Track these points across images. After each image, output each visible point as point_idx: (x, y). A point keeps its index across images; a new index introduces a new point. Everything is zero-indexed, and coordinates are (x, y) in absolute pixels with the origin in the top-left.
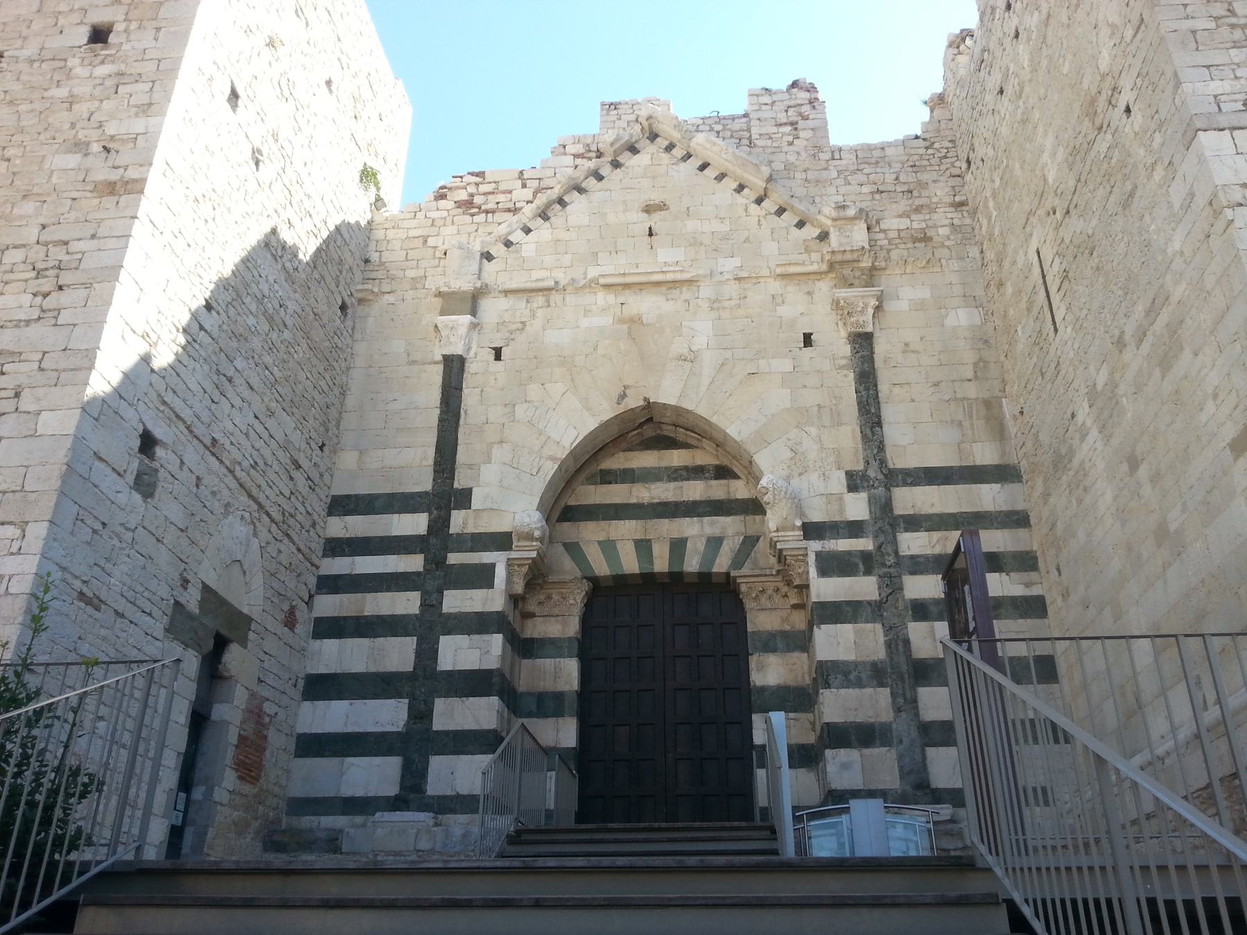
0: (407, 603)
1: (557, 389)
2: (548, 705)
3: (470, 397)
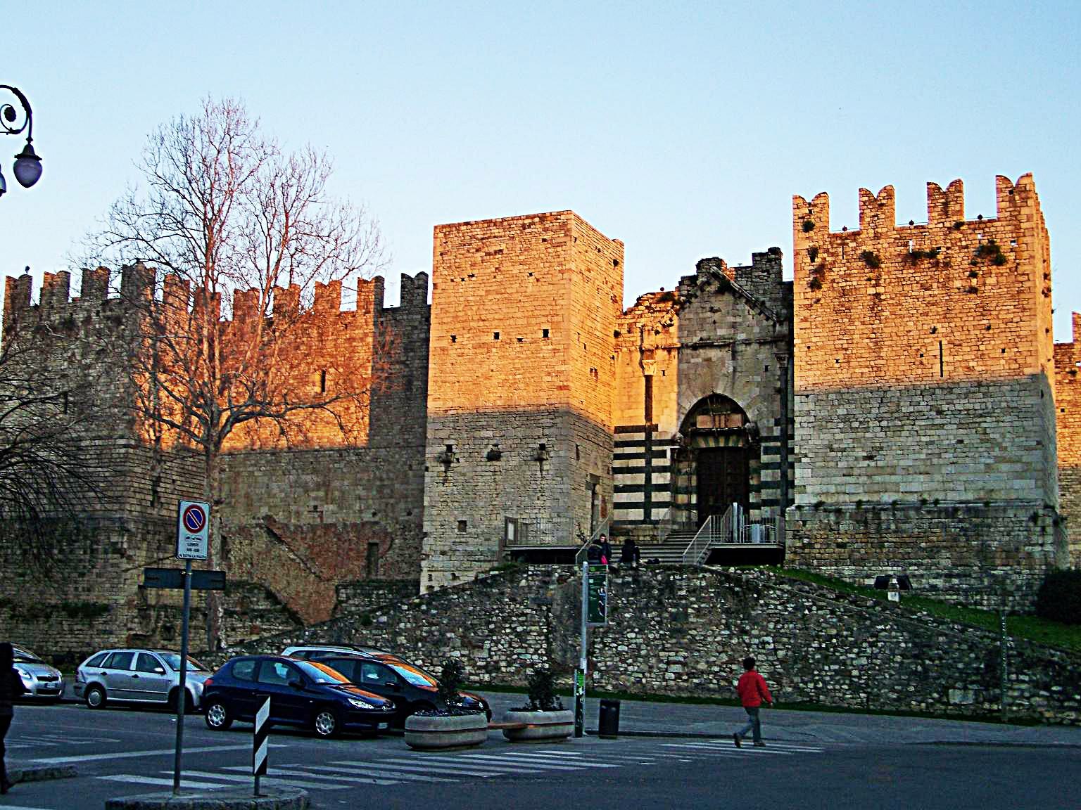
0: (641, 463)
3: (655, 390)
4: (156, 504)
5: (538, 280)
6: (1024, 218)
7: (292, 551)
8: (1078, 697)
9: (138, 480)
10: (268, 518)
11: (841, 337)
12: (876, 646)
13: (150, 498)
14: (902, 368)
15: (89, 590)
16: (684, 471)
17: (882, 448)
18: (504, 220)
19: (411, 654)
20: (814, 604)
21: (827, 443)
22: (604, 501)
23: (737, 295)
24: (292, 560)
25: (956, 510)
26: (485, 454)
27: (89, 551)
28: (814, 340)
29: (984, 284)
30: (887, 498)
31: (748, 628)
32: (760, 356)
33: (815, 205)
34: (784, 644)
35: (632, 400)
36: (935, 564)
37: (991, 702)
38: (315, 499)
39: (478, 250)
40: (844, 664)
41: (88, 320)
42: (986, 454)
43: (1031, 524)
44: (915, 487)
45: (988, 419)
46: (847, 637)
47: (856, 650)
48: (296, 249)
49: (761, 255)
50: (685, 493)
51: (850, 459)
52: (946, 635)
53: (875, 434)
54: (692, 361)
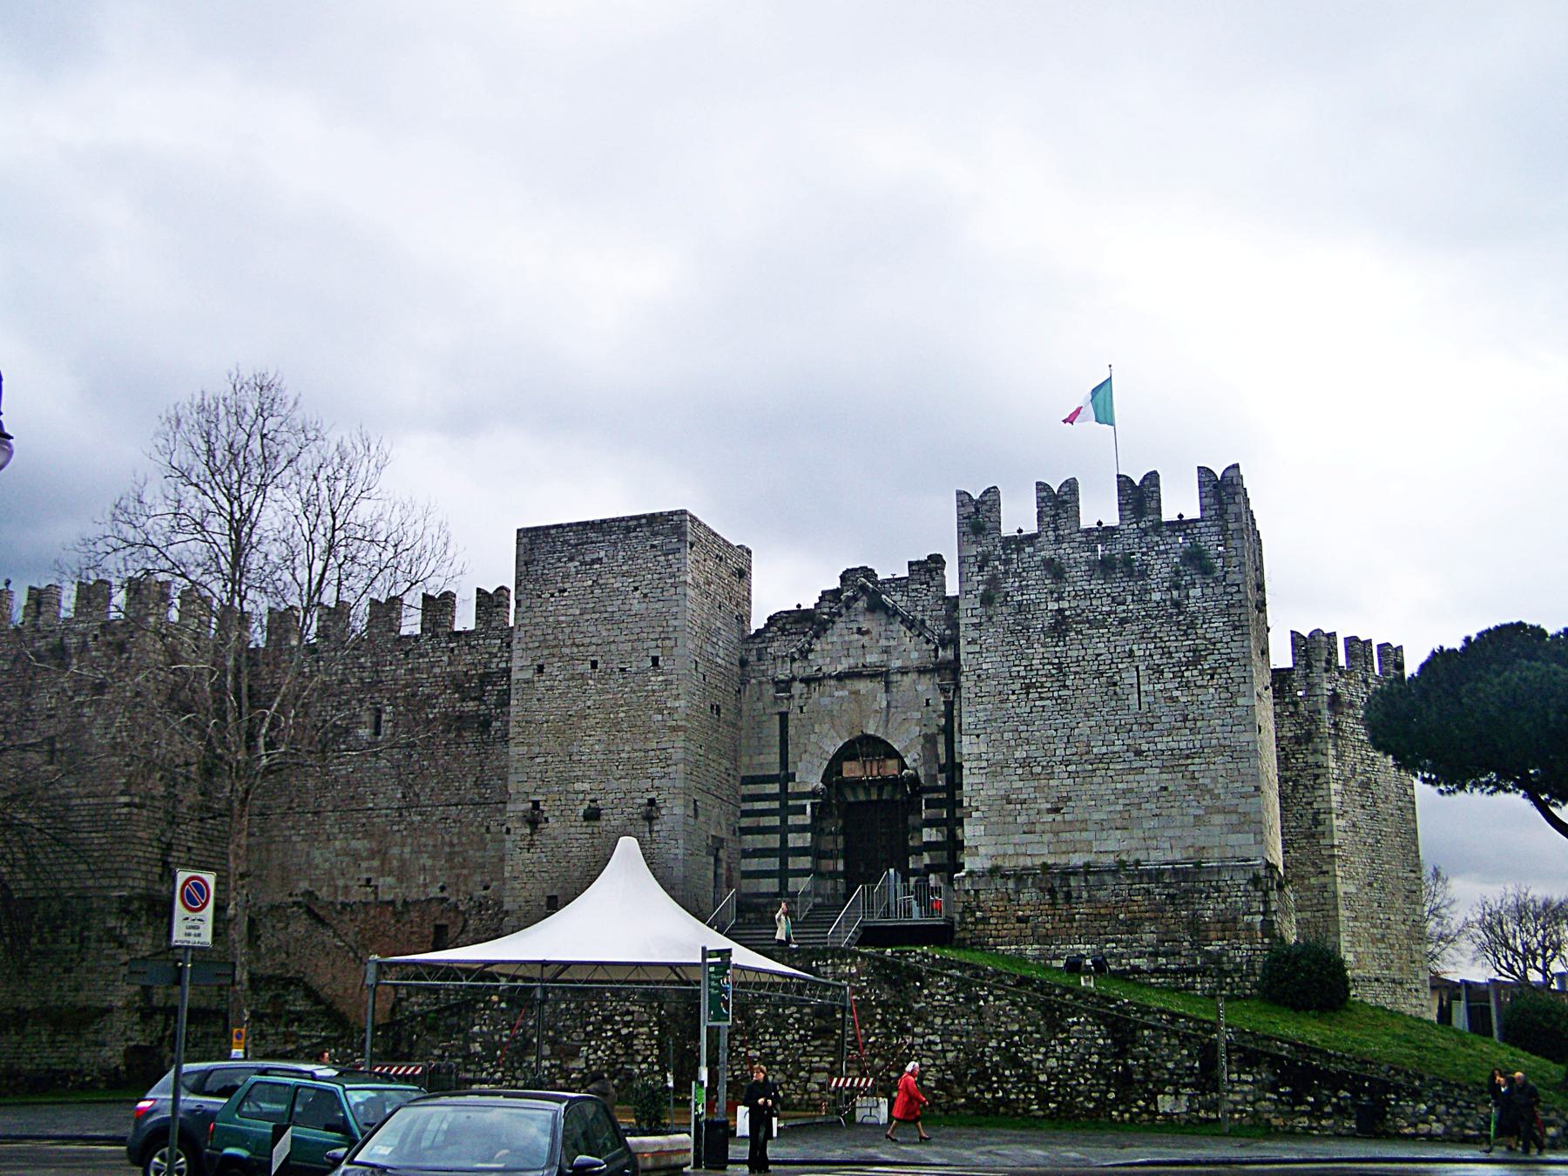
0: (775, 821)
1: (826, 727)
2: (829, 855)
3: (791, 731)
4: (165, 878)
5: (645, 596)
6: (1231, 518)
7: (339, 936)
8: (1311, 1099)
9: (143, 848)
10: (309, 894)
11: (1017, 662)
12: (1068, 1044)
13: (158, 870)
14: (1091, 700)
15: (77, 990)
16: (827, 831)
17: (1070, 799)
18: (603, 521)
19: (487, 1065)
20: (991, 993)
21: (1002, 792)
22: (729, 869)
23: (892, 613)
24: (339, 947)
25: (1161, 873)
26: (581, 813)
27: (77, 940)
28: (985, 666)
29: (1188, 597)
30: (1077, 860)
31: (909, 1024)
32: (919, 688)
33: (984, 503)
34: (954, 1044)
35: (763, 742)
36: (1136, 940)
37: (1208, 1110)
38: (368, 869)
39: (571, 559)
40: (1031, 1068)
41: (84, 647)
42: (1195, 803)
43: (1250, 888)
44: (1111, 845)
45: (1197, 761)
46: (1031, 1033)
47: (1043, 1050)
48: (345, 557)
49: (918, 563)
50: (831, 858)
51: (1030, 812)
52: (1154, 1028)
53: (1061, 782)
54: (836, 694)
